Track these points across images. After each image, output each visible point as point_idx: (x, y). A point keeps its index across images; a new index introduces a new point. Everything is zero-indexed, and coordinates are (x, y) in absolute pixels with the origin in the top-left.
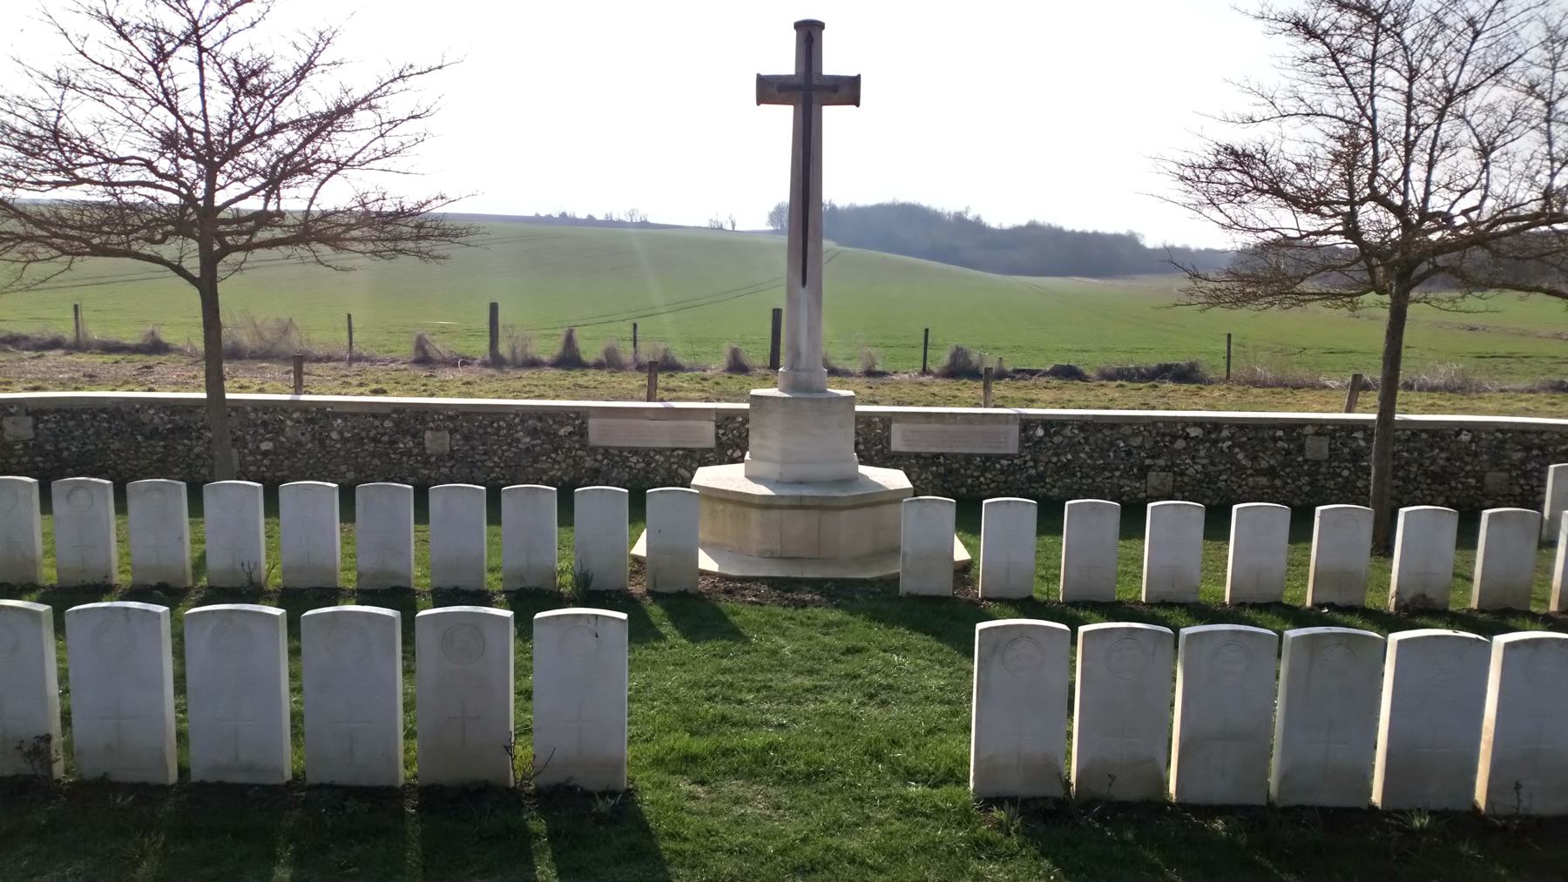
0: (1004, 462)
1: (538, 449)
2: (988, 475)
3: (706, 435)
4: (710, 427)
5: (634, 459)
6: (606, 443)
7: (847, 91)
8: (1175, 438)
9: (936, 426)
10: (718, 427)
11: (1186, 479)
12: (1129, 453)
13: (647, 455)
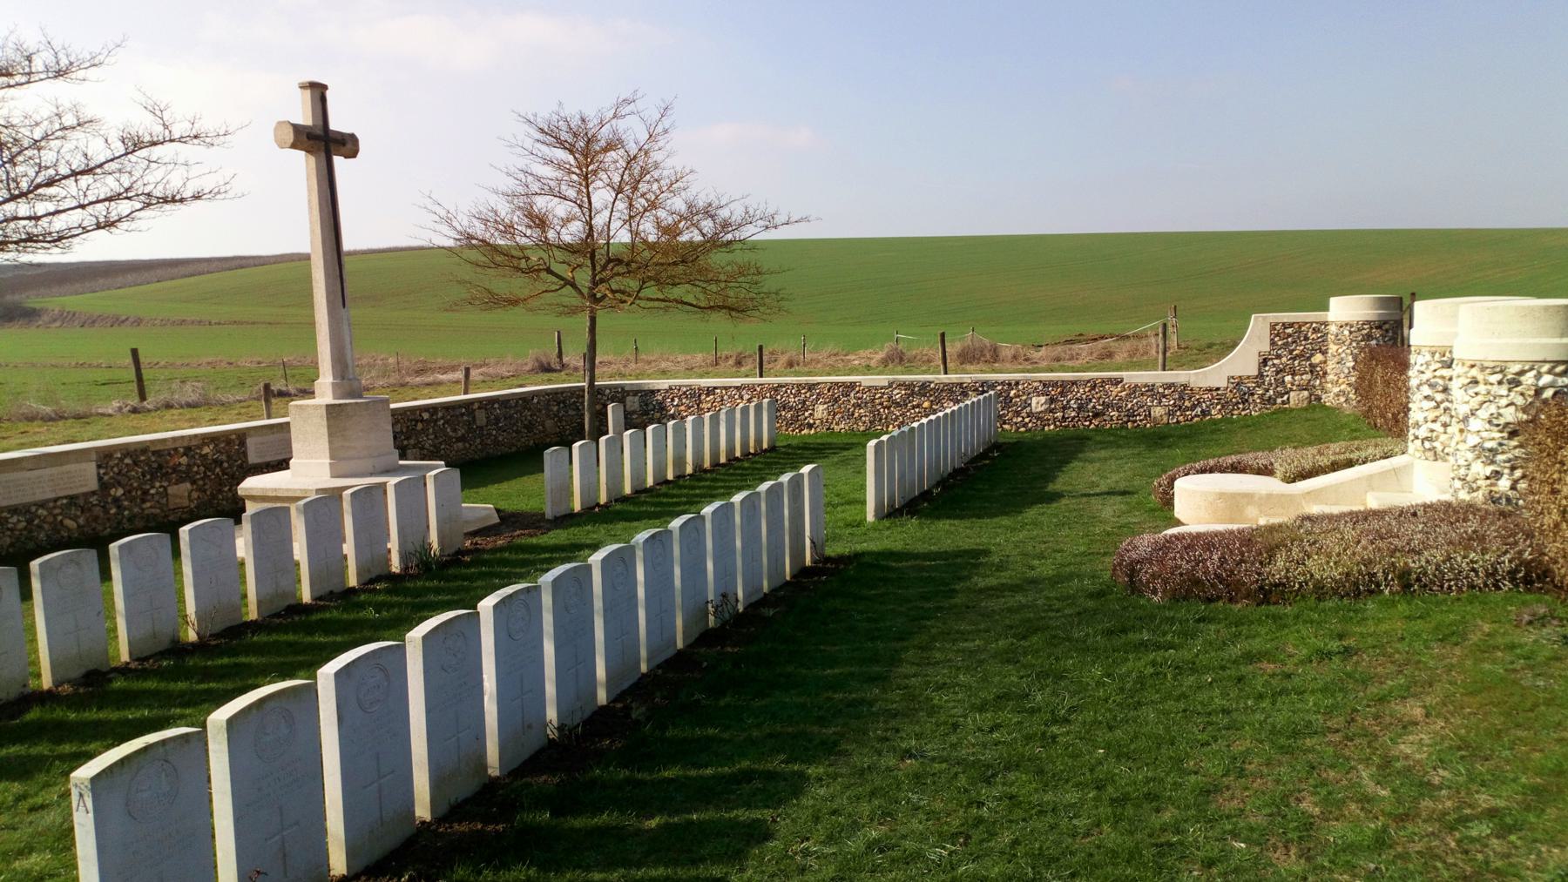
4: (90, 469)
5: (15, 519)
10: (99, 467)
13: (28, 511)
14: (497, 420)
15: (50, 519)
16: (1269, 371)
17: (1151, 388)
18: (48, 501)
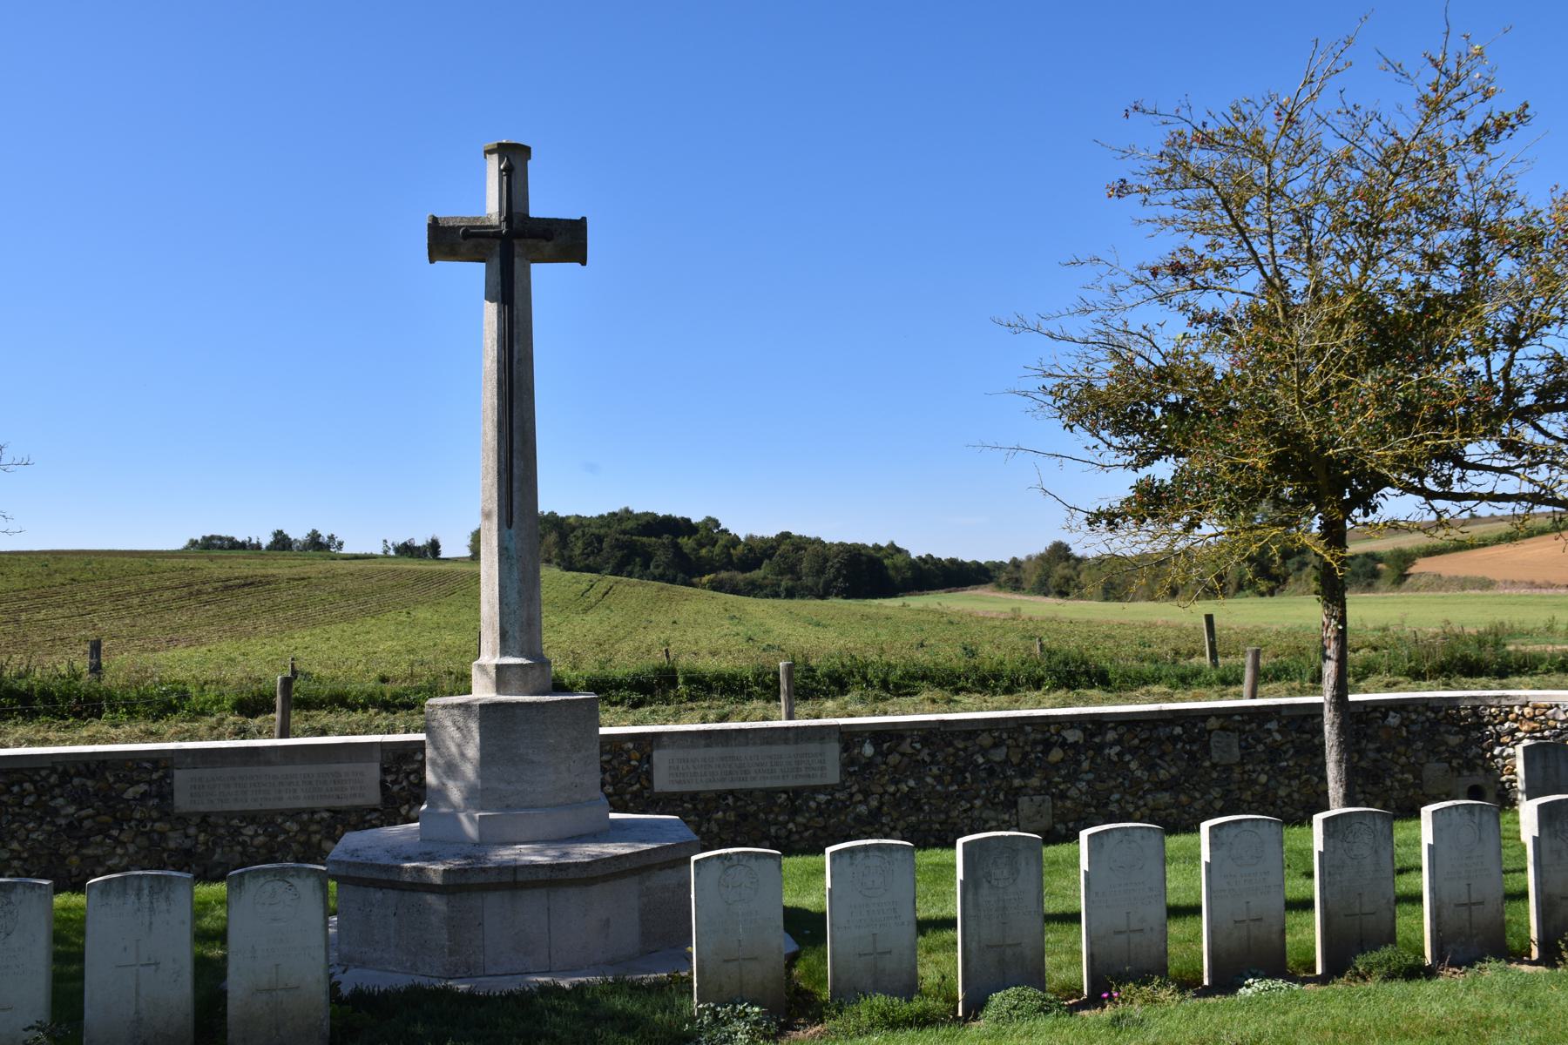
0: (822, 798)
1: (87, 824)
2: (800, 819)
3: (366, 787)
4: (373, 771)
5: (249, 831)
6: (203, 808)
7: (568, 240)
8: (1048, 746)
9: (716, 751)
10: (385, 771)
11: (1068, 804)
12: (991, 772)
14: (1274, 753)
15: (302, 838)
18: (303, 811)
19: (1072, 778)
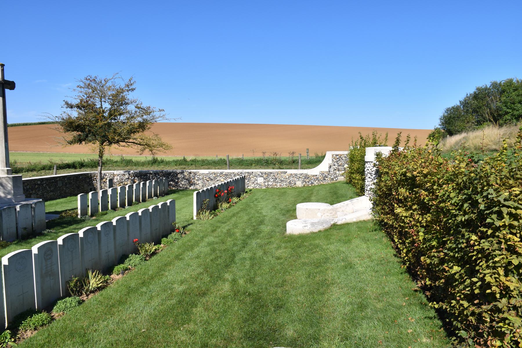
14: (66, 184)
16: (332, 169)
17: (296, 175)
19: (39, 191)
